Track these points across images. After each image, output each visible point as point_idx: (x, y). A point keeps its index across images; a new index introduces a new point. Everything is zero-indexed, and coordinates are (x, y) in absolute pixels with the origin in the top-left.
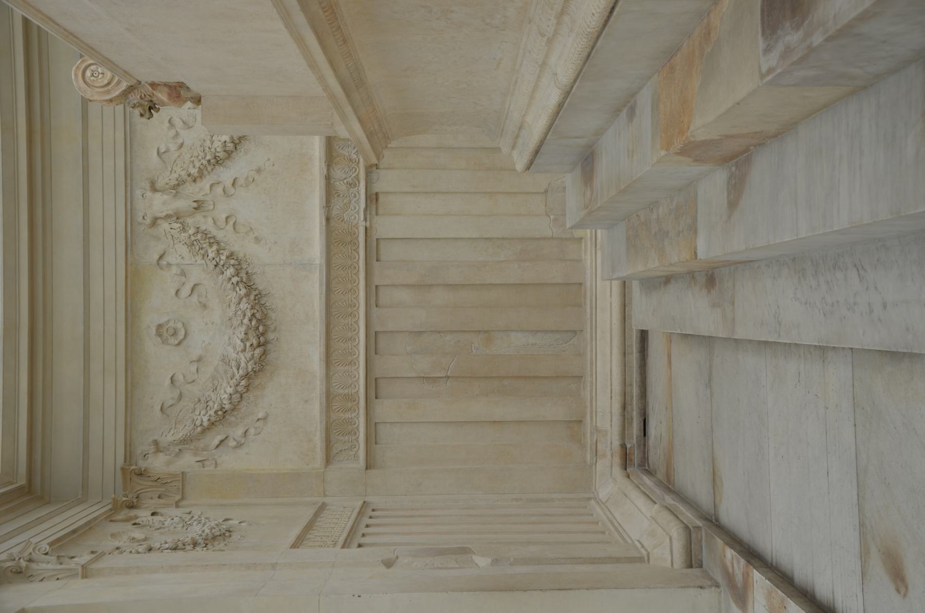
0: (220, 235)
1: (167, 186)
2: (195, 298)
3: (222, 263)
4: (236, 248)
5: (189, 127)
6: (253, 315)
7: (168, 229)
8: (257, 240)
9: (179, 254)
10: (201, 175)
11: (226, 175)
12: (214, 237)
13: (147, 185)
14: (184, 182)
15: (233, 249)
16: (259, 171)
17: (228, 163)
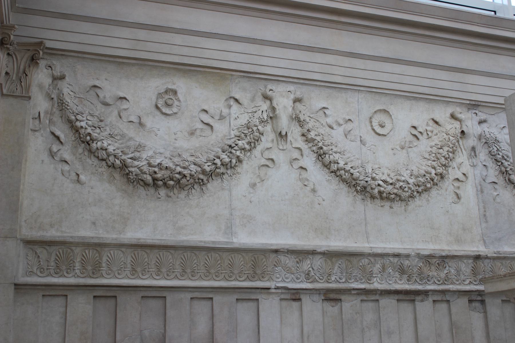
0: (257, 152)
1: (298, 112)
2: (200, 126)
3: (234, 152)
4: (245, 165)
5: (346, 136)
6: (185, 176)
7: (261, 110)
8: (253, 186)
9: (239, 117)
10: (308, 141)
11: (309, 161)
12: (255, 147)
13: (298, 95)
14: (301, 126)
15: (244, 162)
16: (314, 191)
17: (319, 165)
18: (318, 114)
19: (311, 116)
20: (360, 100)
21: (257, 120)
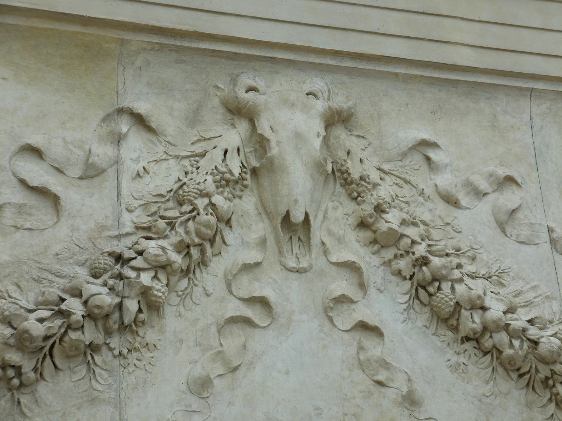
0: (211, 278)
1: (342, 154)
3: (128, 272)
4: (173, 321)
5: (502, 227)
7: (222, 144)
8: (202, 386)
9: (149, 171)
10: (382, 241)
11: (387, 304)
12: (203, 263)
13: (340, 102)
14: (356, 198)
15: (169, 311)
16: (410, 400)
17: (422, 317)
18: (406, 162)
19: (385, 167)
20: (537, 121)
21: (210, 178)
